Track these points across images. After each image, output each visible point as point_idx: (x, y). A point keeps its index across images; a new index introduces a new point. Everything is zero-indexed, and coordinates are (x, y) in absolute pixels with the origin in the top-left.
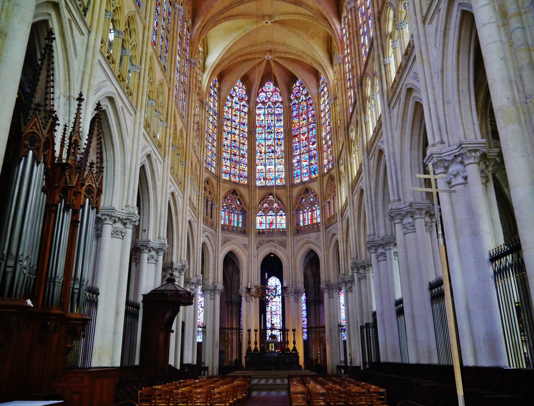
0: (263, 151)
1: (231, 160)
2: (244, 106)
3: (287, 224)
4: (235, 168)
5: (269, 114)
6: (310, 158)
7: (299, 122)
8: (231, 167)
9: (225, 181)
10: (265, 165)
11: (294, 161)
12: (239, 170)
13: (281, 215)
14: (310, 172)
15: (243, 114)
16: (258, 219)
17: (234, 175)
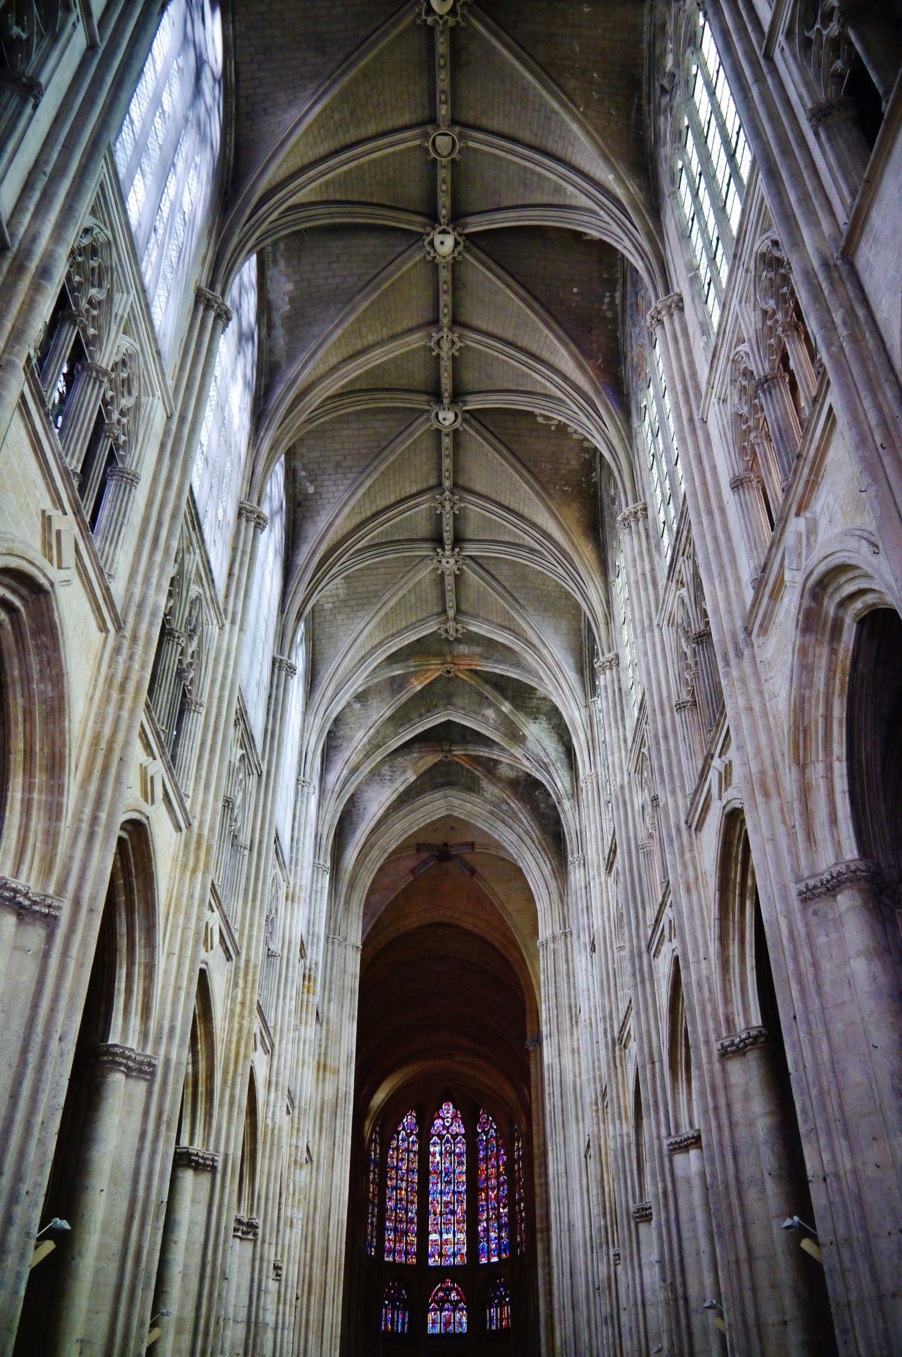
0: (438, 1211)
1: (395, 1230)
2: (413, 1142)
3: (468, 1323)
4: (400, 1241)
5: (446, 1152)
6: (500, 1228)
7: (487, 1169)
8: (395, 1242)
9: (389, 1262)
10: (441, 1235)
11: (480, 1228)
12: (407, 1243)
13: (461, 1310)
14: (499, 1250)
15: (412, 1155)
16: (431, 1316)
17: (400, 1252)
